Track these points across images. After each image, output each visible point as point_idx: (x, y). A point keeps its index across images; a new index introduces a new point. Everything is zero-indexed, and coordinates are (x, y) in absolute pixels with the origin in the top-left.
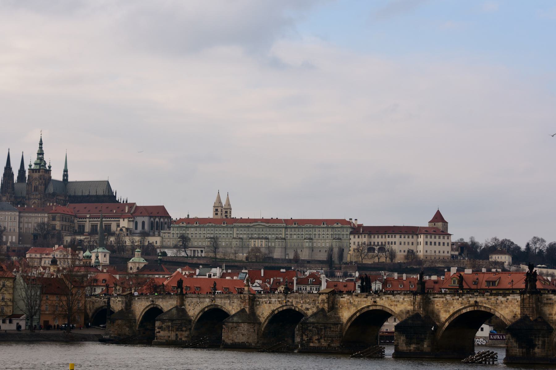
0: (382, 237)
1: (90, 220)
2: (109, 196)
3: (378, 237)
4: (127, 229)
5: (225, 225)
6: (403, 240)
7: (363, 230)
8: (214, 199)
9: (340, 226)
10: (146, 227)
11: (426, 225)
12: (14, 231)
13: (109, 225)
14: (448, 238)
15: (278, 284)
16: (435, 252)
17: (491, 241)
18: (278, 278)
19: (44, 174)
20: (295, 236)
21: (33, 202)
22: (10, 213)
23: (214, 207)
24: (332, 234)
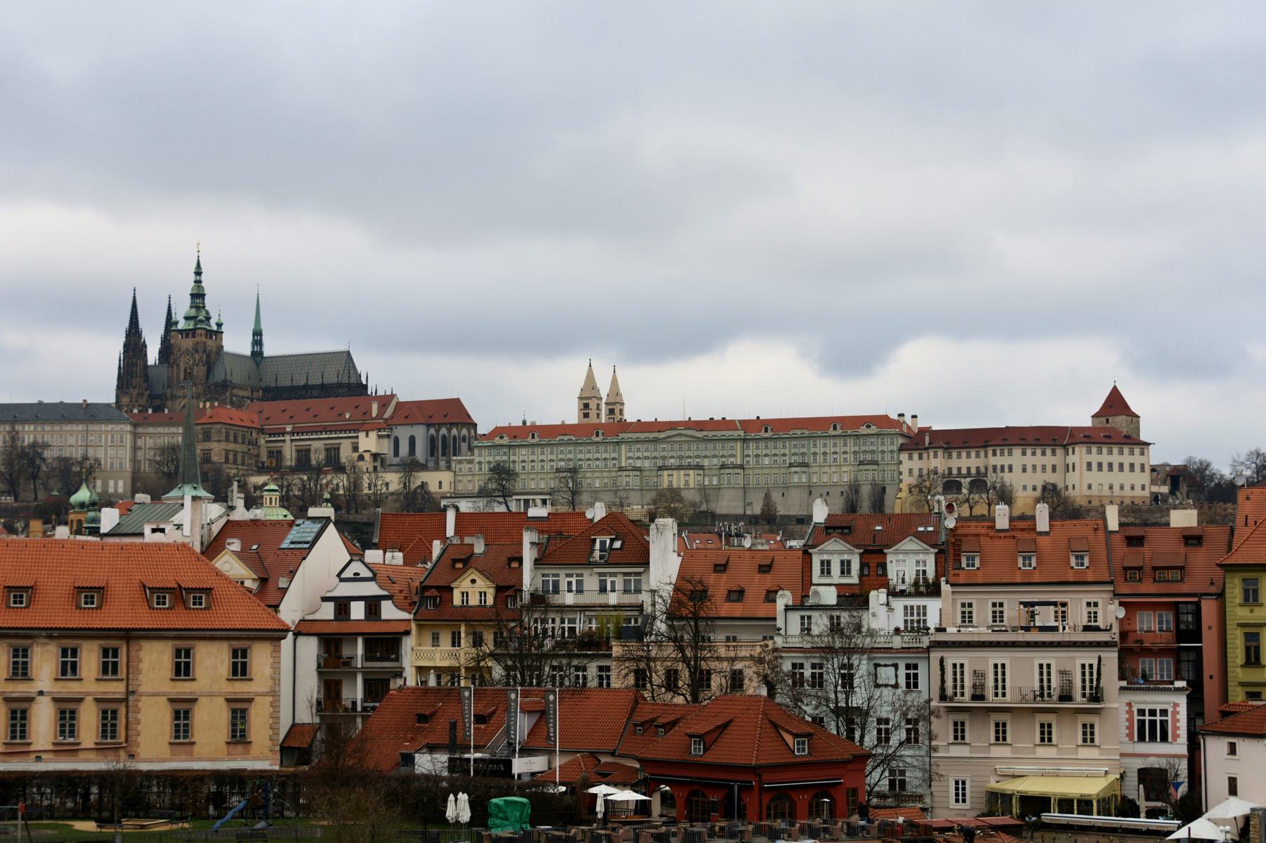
0: (978, 456)
1: (293, 438)
2: (349, 386)
3: (968, 456)
4: (375, 456)
5: (600, 439)
6: (1029, 460)
7: (930, 439)
8: (580, 382)
9: (873, 432)
10: (421, 454)
11: (1090, 424)
12: (121, 467)
13: (335, 449)
14: (1142, 453)
15: (459, 565)
16: (1111, 487)
17: (1248, 459)
18: (468, 540)
19: (203, 339)
20: (767, 461)
21: (182, 404)
22: (110, 427)
23: (580, 398)
24: (855, 452)
